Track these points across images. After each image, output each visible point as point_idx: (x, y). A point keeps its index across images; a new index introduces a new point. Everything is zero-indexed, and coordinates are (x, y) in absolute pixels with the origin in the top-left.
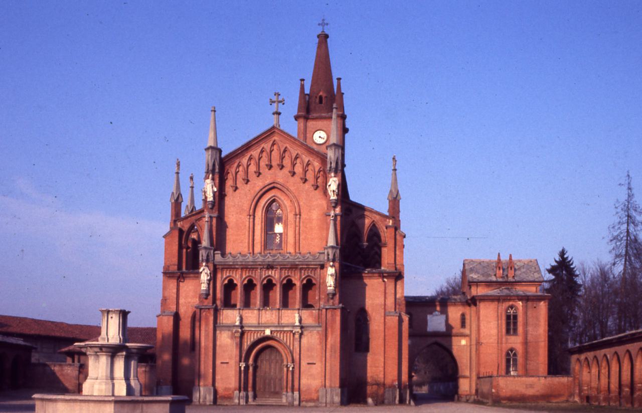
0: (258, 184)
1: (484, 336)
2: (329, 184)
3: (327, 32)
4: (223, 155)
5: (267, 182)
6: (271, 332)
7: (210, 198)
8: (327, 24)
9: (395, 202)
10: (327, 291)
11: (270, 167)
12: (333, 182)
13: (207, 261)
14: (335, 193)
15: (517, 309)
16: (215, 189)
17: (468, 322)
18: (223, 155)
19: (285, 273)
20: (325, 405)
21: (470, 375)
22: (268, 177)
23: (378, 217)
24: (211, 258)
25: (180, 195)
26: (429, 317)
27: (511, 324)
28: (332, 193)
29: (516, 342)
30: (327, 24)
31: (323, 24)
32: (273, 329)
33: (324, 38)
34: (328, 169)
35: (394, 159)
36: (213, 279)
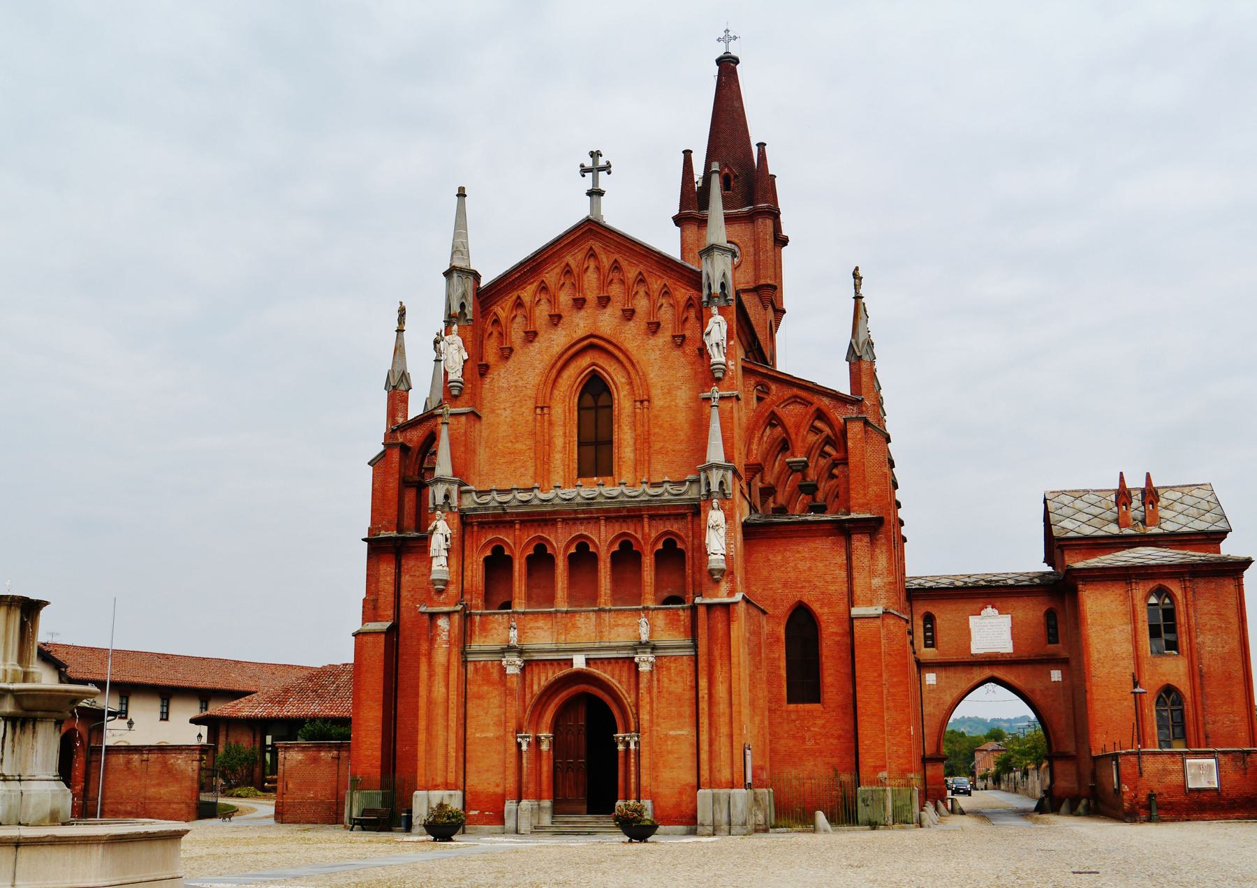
0: (557, 341)
1: (1099, 659)
2: (707, 330)
3: (734, 54)
4: (484, 282)
5: (580, 333)
6: (588, 661)
7: (456, 375)
8: (735, 38)
9: (860, 359)
11: (579, 303)
12: (716, 326)
15: (1171, 596)
16: (466, 357)
18: (484, 282)
19: (617, 529)
20: (711, 828)
21: (1077, 749)
22: (580, 324)
23: (826, 401)
24: (454, 501)
25: (404, 377)
26: (973, 620)
27: (1165, 629)
28: (715, 348)
29: (1173, 669)
30: (735, 38)
31: (727, 38)
32: (593, 655)
33: (727, 65)
34: (705, 299)
35: (856, 276)
36: (457, 550)
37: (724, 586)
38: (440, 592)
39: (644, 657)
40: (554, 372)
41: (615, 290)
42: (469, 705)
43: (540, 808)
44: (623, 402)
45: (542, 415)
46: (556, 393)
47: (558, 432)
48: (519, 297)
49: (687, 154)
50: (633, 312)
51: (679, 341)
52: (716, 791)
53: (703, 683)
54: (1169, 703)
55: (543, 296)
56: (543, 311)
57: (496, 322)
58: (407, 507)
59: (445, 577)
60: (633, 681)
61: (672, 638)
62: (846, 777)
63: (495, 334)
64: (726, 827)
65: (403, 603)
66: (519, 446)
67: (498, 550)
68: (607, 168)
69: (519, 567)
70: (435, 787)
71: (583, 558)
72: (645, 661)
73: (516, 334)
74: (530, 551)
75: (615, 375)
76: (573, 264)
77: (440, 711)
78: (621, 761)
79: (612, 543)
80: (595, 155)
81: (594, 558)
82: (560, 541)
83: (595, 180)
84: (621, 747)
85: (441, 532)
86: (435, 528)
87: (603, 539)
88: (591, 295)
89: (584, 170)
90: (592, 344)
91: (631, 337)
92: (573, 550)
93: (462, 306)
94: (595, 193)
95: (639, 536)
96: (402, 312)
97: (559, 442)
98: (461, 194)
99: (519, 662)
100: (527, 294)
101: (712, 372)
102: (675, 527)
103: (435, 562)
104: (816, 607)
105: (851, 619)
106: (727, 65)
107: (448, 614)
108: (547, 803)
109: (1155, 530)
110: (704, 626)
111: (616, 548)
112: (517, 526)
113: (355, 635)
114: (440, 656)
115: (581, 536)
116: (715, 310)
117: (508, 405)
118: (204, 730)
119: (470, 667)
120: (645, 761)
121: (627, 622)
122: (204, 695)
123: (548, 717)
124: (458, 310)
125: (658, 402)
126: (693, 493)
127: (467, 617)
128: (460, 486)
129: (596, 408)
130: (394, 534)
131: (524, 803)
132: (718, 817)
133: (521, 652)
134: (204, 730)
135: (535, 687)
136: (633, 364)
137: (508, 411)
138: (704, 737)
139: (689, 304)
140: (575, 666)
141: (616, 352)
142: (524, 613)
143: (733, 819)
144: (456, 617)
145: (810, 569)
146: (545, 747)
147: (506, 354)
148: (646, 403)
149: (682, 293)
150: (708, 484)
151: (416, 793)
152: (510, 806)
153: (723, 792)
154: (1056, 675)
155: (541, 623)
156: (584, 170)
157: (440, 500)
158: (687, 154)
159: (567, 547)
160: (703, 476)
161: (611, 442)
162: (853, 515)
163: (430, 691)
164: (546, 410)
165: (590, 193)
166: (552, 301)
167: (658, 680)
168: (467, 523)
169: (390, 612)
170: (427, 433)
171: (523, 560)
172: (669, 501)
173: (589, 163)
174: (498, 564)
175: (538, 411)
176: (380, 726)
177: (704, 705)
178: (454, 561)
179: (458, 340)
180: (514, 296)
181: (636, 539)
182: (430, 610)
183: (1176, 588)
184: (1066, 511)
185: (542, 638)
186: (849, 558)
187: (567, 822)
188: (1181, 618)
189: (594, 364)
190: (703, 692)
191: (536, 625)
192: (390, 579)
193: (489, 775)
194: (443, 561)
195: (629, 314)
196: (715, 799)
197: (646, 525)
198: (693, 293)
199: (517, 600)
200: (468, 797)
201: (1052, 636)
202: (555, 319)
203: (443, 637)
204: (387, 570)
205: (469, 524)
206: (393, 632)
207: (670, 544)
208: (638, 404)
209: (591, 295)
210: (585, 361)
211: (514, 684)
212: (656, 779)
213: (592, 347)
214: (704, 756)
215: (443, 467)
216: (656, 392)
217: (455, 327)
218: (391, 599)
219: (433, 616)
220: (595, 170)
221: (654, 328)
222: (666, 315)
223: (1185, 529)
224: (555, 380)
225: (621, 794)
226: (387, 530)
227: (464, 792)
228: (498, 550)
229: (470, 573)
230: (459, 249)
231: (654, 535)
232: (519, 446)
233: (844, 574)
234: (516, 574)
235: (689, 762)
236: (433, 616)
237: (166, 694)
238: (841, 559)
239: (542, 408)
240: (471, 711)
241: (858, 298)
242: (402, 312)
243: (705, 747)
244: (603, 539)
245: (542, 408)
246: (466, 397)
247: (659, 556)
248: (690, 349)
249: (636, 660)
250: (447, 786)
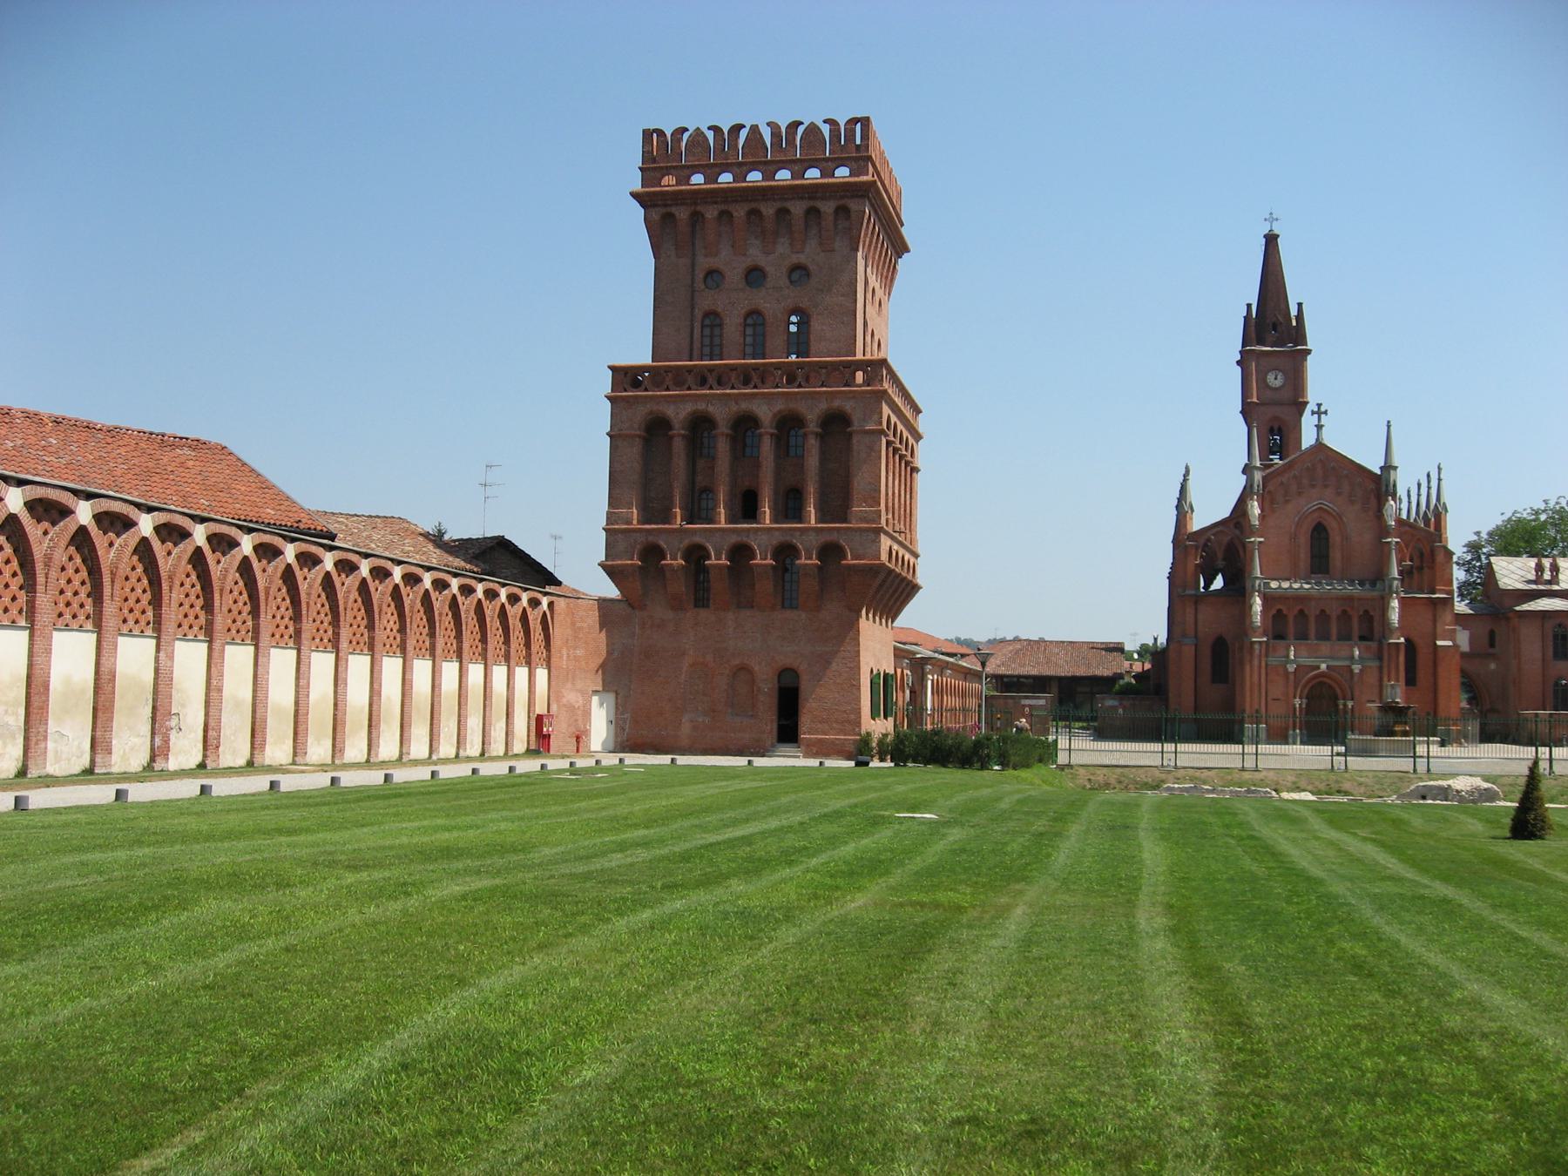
11: (1313, 486)
31: (1272, 219)
33: (1271, 240)
44: (1335, 538)
49: (1249, 306)
67: (1279, 611)
72: (1356, 668)
75: (1332, 525)
80: (1319, 405)
82: (1312, 612)
106: (1271, 240)
109: (1556, 587)
110: (1381, 654)
114: (1256, 662)
154: (1493, 666)
158: (1249, 306)
168: (1267, 600)
201: (1492, 645)
211: (1292, 677)
244: (1334, 611)
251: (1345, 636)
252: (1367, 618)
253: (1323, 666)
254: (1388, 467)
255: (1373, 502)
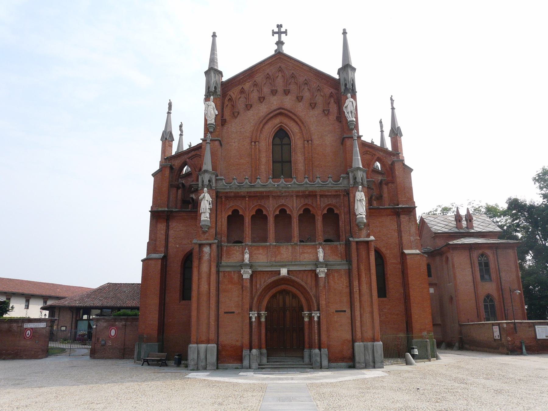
0: (263, 110)
2: (345, 105)
5: (274, 107)
10: (356, 221)
11: (274, 92)
13: (210, 187)
14: (353, 114)
15: (487, 256)
16: (217, 113)
17: (433, 271)
18: (224, 79)
20: (364, 365)
22: (274, 102)
23: (381, 153)
28: (350, 114)
29: (489, 288)
32: (292, 268)
34: (343, 90)
35: (391, 99)
37: (364, 232)
38: (204, 233)
39: (322, 269)
40: (262, 125)
41: (293, 87)
42: (221, 295)
43: (261, 354)
44: (297, 141)
45: (255, 145)
46: (262, 136)
47: (263, 155)
48: (242, 88)
50: (302, 97)
51: (326, 112)
52: (365, 343)
53: (356, 283)
54: (488, 301)
55: (255, 89)
56: (255, 95)
57: (230, 100)
58: (171, 197)
59: (209, 224)
60: (314, 283)
61: (334, 259)
62: (402, 335)
63: (229, 106)
64: (372, 364)
65: (170, 245)
66: (242, 161)
67: (235, 212)
68: (285, 32)
69: (247, 220)
70: (202, 342)
71: (283, 216)
72: (322, 272)
73: (241, 105)
74: (253, 213)
75: (292, 128)
76: (270, 73)
77: (204, 298)
78: (306, 327)
79: (300, 209)
81: (289, 217)
82: (271, 208)
83: (280, 37)
84: (306, 320)
85: (206, 202)
86: (204, 197)
87: (295, 208)
88: (280, 89)
89: (274, 33)
90: (281, 112)
91: (301, 109)
92: (277, 213)
93: (215, 88)
94: (280, 43)
95: (314, 205)
96: (170, 105)
97: (264, 160)
98: (214, 36)
99: (250, 271)
100: (247, 86)
101: (349, 127)
102: (334, 201)
103: (203, 215)
104: (383, 250)
105: (403, 255)
107: (210, 245)
108: (264, 351)
109: (473, 231)
111: (301, 212)
112: (247, 199)
113: (142, 261)
114: (205, 268)
115: (283, 205)
116: (349, 95)
117: (236, 140)
118: (47, 312)
119: (221, 274)
120: (324, 327)
121: (309, 251)
122: (45, 298)
123: (265, 303)
124: (214, 89)
125: (316, 142)
126: (343, 184)
127: (220, 247)
128: (217, 176)
129: (282, 145)
130: (166, 209)
131: (254, 351)
132: (367, 358)
133: (251, 266)
134: (47, 312)
135: (258, 286)
136: (303, 123)
137: (236, 144)
138: (357, 313)
139: (331, 96)
140: (281, 275)
141: (294, 117)
142: (251, 246)
143: (376, 359)
144: (214, 247)
145: (380, 231)
146: (263, 320)
147: (235, 115)
148: (310, 142)
149: (328, 90)
150: (355, 178)
151: (191, 345)
152: (246, 352)
153: (370, 344)
155: (261, 251)
156: (274, 33)
157: (206, 182)
159: (275, 211)
160: (351, 175)
161: (290, 162)
162: (400, 206)
163: (199, 288)
164: (257, 143)
165: (277, 43)
166: (260, 91)
167: (328, 283)
169: (163, 249)
170: (183, 161)
171: (250, 217)
172: (332, 187)
173: (276, 30)
174: (235, 219)
175: (253, 143)
176: (158, 308)
177: (356, 296)
178: (214, 215)
179: (213, 104)
180: (240, 87)
181: (313, 207)
182: (199, 242)
183: (489, 252)
184: (432, 223)
185: (263, 260)
186: (399, 226)
187: (277, 362)
188: (492, 265)
189: (281, 123)
190: (356, 289)
191: (258, 252)
192: (163, 232)
193: (233, 334)
194: (208, 215)
195: (299, 99)
196: (365, 348)
197: (318, 200)
198: (332, 90)
199: (247, 238)
200: (220, 348)
202: (262, 99)
203: (206, 257)
204: (162, 227)
205: (219, 198)
206: (165, 259)
207: (330, 211)
208: (306, 142)
209: (280, 89)
210: (277, 121)
212: (328, 337)
213: (280, 114)
214: (358, 324)
215: (207, 165)
216: (315, 137)
217: (212, 97)
218: (163, 242)
219: (201, 246)
220: (280, 33)
221: (313, 106)
222: (319, 99)
223: (484, 231)
224: (261, 130)
225: (307, 345)
226: (161, 207)
227: (218, 345)
228: (235, 212)
229: (220, 223)
230: (213, 60)
231: (323, 205)
232: (242, 161)
233: (396, 234)
234: (247, 224)
235: (348, 328)
236: (201, 246)
237: (28, 298)
238: (395, 227)
239: (255, 142)
240: (222, 299)
241: (393, 109)
242: (170, 105)
243: (358, 318)
244: (295, 208)
245: (255, 142)
246: (217, 133)
247: (324, 216)
248: (333, 117)
249: (318, 271)
250: (208, 342)
251: (308, 238)
252: (331, 216)
253: (284, 272)
254: (347, 67)
255: (333, 108)
